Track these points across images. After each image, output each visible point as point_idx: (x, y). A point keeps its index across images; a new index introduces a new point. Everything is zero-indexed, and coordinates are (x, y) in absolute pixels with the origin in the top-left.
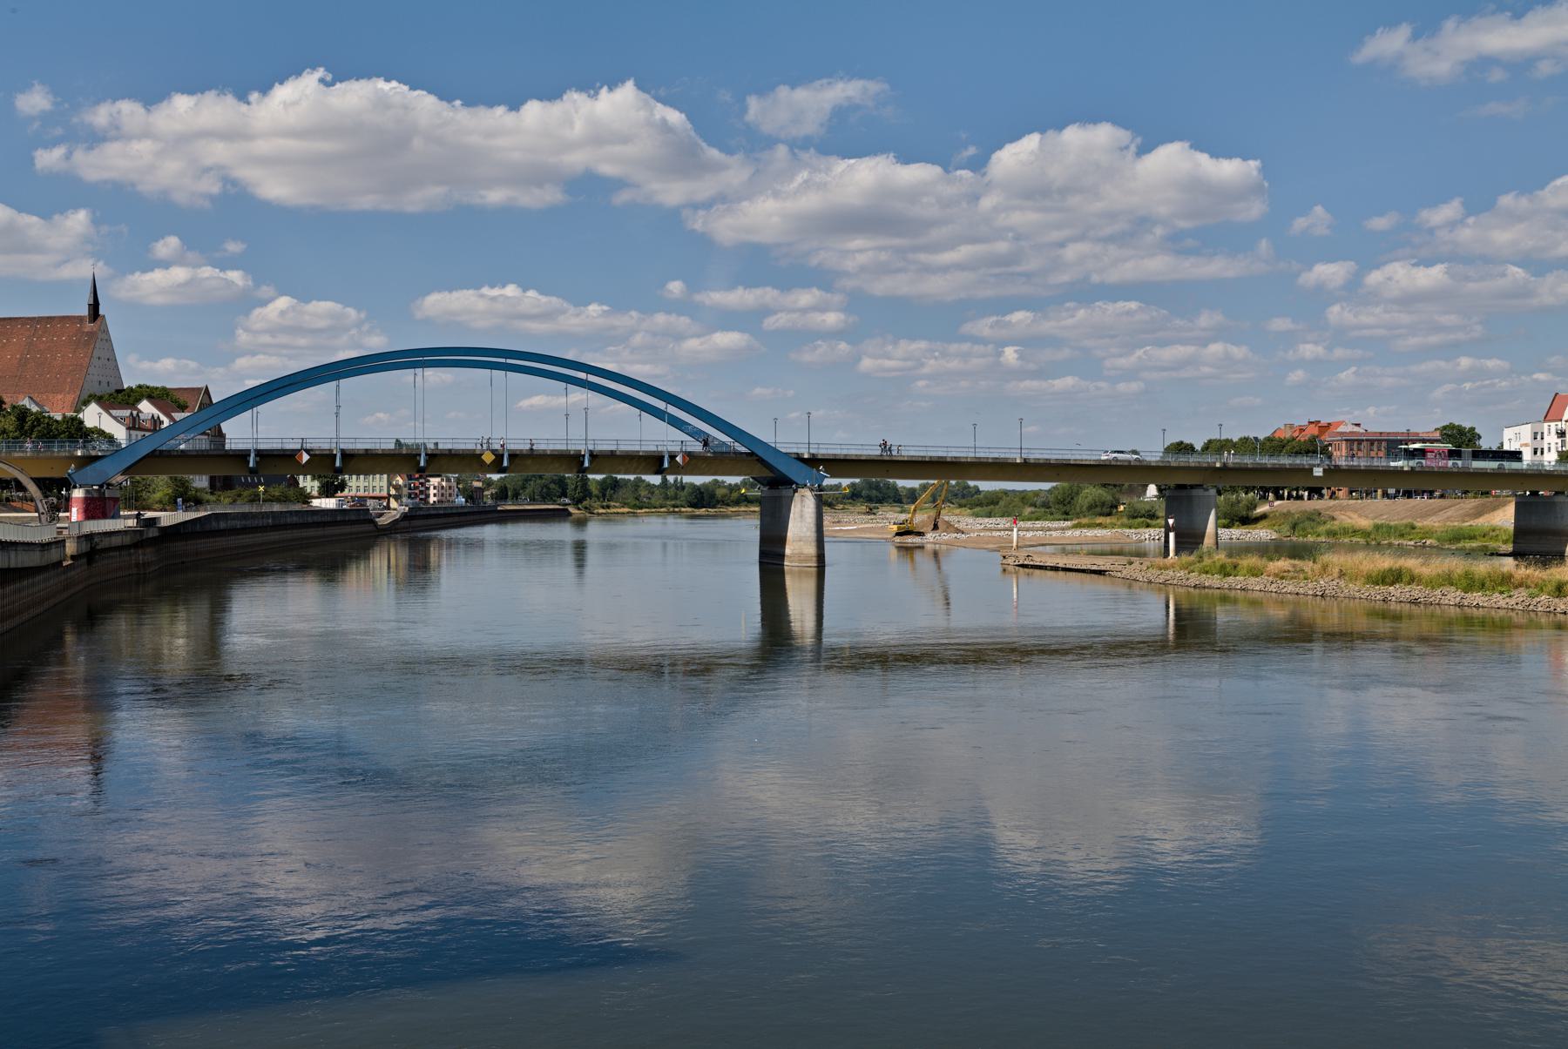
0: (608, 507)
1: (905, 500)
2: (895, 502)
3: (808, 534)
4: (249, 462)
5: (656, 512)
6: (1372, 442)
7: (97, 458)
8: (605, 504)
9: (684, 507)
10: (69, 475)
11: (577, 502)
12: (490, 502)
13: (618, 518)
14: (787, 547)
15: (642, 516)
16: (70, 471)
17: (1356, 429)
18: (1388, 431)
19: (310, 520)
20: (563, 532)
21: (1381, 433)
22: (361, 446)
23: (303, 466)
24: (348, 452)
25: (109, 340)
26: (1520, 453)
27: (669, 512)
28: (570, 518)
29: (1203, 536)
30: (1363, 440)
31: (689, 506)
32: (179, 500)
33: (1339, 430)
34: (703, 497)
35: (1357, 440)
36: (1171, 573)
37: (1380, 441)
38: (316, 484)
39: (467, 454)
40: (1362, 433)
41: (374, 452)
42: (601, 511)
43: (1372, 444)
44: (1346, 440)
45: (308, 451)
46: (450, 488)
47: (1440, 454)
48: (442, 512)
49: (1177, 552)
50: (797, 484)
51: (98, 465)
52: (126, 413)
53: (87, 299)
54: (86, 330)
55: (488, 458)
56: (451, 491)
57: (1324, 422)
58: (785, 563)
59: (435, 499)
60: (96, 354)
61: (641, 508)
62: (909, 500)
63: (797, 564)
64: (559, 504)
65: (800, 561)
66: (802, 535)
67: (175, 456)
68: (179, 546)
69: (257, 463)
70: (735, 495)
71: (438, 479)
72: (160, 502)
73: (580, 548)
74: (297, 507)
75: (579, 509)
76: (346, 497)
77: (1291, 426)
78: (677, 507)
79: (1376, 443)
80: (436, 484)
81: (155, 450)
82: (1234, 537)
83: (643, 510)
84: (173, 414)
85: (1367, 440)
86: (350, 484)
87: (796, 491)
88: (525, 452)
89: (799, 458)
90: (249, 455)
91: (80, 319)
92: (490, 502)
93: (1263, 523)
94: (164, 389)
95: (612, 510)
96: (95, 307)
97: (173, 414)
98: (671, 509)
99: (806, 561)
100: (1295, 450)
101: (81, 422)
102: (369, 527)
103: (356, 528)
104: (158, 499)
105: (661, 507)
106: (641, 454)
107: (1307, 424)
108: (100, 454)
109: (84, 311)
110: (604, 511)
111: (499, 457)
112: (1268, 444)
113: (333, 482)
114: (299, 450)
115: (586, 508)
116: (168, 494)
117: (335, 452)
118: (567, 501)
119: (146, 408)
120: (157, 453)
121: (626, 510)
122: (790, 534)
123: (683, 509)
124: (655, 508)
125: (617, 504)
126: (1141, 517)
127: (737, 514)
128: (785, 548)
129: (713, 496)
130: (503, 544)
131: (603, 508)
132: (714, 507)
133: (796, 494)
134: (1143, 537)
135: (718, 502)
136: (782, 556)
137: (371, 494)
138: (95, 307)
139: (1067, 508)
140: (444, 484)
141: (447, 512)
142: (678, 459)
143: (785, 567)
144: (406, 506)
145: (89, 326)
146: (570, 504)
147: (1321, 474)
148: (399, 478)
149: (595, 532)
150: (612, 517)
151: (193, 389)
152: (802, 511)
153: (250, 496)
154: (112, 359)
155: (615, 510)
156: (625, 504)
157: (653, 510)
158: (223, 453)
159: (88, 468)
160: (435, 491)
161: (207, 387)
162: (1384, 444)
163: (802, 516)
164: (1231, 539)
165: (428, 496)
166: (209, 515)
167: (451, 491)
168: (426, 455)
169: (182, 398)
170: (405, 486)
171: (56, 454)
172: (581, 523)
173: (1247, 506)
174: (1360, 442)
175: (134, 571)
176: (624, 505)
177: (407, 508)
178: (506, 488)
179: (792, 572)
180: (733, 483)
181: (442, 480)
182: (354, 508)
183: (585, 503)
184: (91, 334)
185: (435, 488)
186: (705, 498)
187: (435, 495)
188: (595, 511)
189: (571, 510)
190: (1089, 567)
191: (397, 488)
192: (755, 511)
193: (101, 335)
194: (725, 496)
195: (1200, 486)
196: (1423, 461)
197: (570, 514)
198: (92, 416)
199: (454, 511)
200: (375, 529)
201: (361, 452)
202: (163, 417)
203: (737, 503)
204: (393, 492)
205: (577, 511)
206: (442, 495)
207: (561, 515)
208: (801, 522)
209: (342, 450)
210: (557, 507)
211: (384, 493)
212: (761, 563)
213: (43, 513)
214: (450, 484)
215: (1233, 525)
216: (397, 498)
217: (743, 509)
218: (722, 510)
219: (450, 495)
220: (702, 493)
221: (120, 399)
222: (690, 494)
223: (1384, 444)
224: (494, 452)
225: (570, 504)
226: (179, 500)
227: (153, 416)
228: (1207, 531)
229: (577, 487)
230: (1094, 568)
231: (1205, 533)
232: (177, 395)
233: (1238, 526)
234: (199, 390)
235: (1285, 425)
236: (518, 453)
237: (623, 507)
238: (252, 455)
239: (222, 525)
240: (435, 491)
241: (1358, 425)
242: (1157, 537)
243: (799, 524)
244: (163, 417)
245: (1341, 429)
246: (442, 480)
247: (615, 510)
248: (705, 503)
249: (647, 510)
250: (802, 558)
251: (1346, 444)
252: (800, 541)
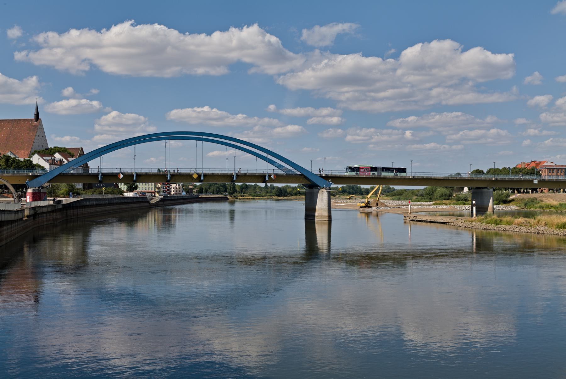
0: (243, 196)
1: (364, 193)
2: (360, 194)
3: (325, 207)
4: (99, 178)
5: (263, 198)
6: (558, 169)
7: (37, 176)
8: (242, 195)
9: (274, 196)
10: (26, 183)
11: (231, 194)
12: (196, 194)
13: (248, 200)
14: (316, 212)
15: (257, 200)
16: (26, 181)
17: (552, 164)
19: (123, 201)
20: (225, 206)
21: (562, 166)
22: (144, 171)
23: (121, 179)
24: (139, 174)
25: (43, 129)
26: (405, 169)
27: (268, 198)
28: (228, 201)
29: (487, 208)
30: (555, 169)
31: (276, 196)
32: (71, 193)
33: (544, 164)
34: (282, 192)
36: (474, 223)
37: (562, 169)
38: (126, 187)
39: (186, 175)
40: (554, 166)
41: (149, 174)
42: (241, 198)
43: (558, 170)
44: (547, 169)
45: (122, 173)
46: (180, 188)
47: (367, 169)
48: (176, 198)
49: (476, 215)
50: (320, 187)
51: (38, 179)
52: (49, 158)
53: (34, 112)
54: (34, 125)
55: (195, 176)
56: (180, 190)
57: (538, 161)
58: (315, 219)
59: (174, 193)
60: (37, 134)
61: (257, 197)
62: (366, 193)
63: (320, 219)
64: (224, 195)
65: (321, 218)
66: (322, 208)
67: (69, 176)
68: (71, 212)
69: (102, 178)
70: (295, 191)
71: (175, 185)
72: (63, 194)
73: (232, 212)
74: (118, 196)
75: (232, 197)
76: (138, 192)
77: (524, 163)
78: (271, 196)
79: (560, 170)
80: (174, 187)
81: (61, 173)
82: (500, 208)
83: (258, 198)
84: (68, 159)
85: (556, 169)
86: (139, 187)
87: (319, 190)
88: (210, 174)
89: (321, 176)
90: (99, 175)
91: (31, 120)
92: (196, 194)
93: (513, 203)
94: (65, 148)
95: (245, 197)
96: (37, 115)
97: (68, 159)
98: (269, 197)
99: (324, 218)
100: (526, 173)
101: (31, 162)
102: (147, 204)
103: (142, 205)
104: (62, 193)
105: (265, 196)
106: (257, 174)
107: (531, 162)
108: (39, 175)
109: (33, 117)
111: (199, 176)
112: (514, 170)
113: (133, 186)
114: (119, 173)
115: (234, 197)
116: (66, 191)
117: (133, 174)
118: (227, 193)
119: (58, 156)
120: (62, 174)
121: (251, 197)
122: (317, 207)
123: (274, 197)
124: (262, 196)
125: (247, 195)
126: (461, 200)
127: (296, 199)
128: (315, 213)
129: (286, 191)
130: (201, 211)
131: (241, 196)
132: (286, 196)
133: (320, 191)
134: (462, 209)
135: (288, 194)
136: (314, 216)
137: (148, 191)
138: (37, 115)
139: (431, 197)
140: (177, 187)
141: (178, 198)
142: (272, 177)
143: (316, 221)
144: (162, 195)
145: (35, 123)
146: (228, 195)
147: (537, 183)
148: (159, 184)
149: (238, 206)
150: (245, 200)
151: (76, 148)
152: (322, 198)
153: (99, 191)
154: (44, 136)
155: (246, 197)
156: (250, 195)
157: (262, 197)
158: (88, 174)
159: (34, 180)
160: (174, 190)
161: (82, 148)
162: (563, 170)
163: (322, 200)
164: (499, 209)
165: (171, 192)
166: (82, 199)
167: (180, 190)
168: (170, 175)
169: (72, 152)
170: (162, 188)
171: (21, 175)
172: (232, 203)
173: (506, 196)
174: (553, 169)
175: (52, 222)
176: (250, 195)
177: (162, 197)
178: (202, 188)
179: (318, 223)
180: (294, 186)
181: (177, 185)
182: (141, 196)
183: (234, 194)
184: (36, 126)
185: (173, 188)
186: (283, 193)
187: (173, 191)
188: (238, 198)
189: (229, 197)
190: (440, 221)
191: (158, 188)
192: (303, 198)
193: (39, 127)
194: (291, 191)
195: (486, 188)
196: (359, 173)
197: (228, 199)
198: (36, 159)
199: (181, 198)
200: (150, 205)
201: (144, 174)
202: (64, 160)
203: (296, 194)
204: (157, 190)
205: (231, 198)
206: (177, 191)
207: (224, 199)
208: (322, 202)
209: (137, 174)
210: (223, 196)
211: (153, 190)
212: (306, 219)
213: (16, 199)
214: (180, 187)
215: (500, 203)
216: (158, 192)
217: (298, 197)
218: (289, 197)
219: (180, 191)
220: (282, 190)
221: (47, 152)
222: (277, 191)
223: (563, 170)
224: (197, 174)
225: (228, 195)
226: (71, 193)
227: (60, 159)
228: (489, 206)
229: (231, 188)
230: (442, 221)
231: (488, 207)
232: (70, 151)
234: (79, 149)
236: (207, 174)
237: (249, 196)
238: (100, 175)
239: (88, 203)
240: (174, 190)
241: (552, 162)
242: (468, 209)
243: (321, 203)
244: (64, 160)
245: (545, 164)
246: (177, 185)
247: (246, 197)
248: (282, 194)
249: (259, 197)
250: (322, 217)
251: (548, 170)
252: (321, 210)
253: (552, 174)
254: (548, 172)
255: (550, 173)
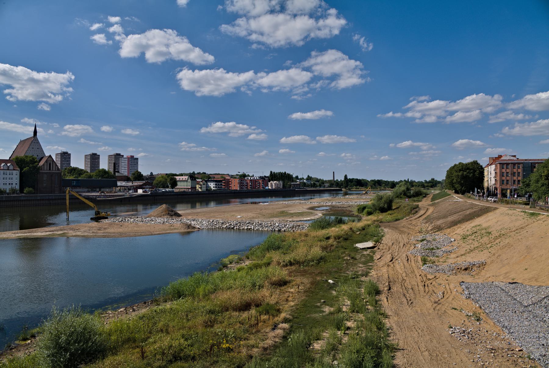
0: (358, 188)
17: (514, 158)
18: (538, 159)
35: (505, 163)
37: (519, 163)
44: (499, 163)
71: (276, 182)
79: (516, 165)
85: (511, 163)
110: (355, 189)
131: (356, 188)
188: (351, 190)
189: (343, 189)
223: (521, 166)
233: (378, 213)
235: (490, 158)
251: (500, 165)
253: (506, 170)
254: (500, 167)
255: (503, 168)
